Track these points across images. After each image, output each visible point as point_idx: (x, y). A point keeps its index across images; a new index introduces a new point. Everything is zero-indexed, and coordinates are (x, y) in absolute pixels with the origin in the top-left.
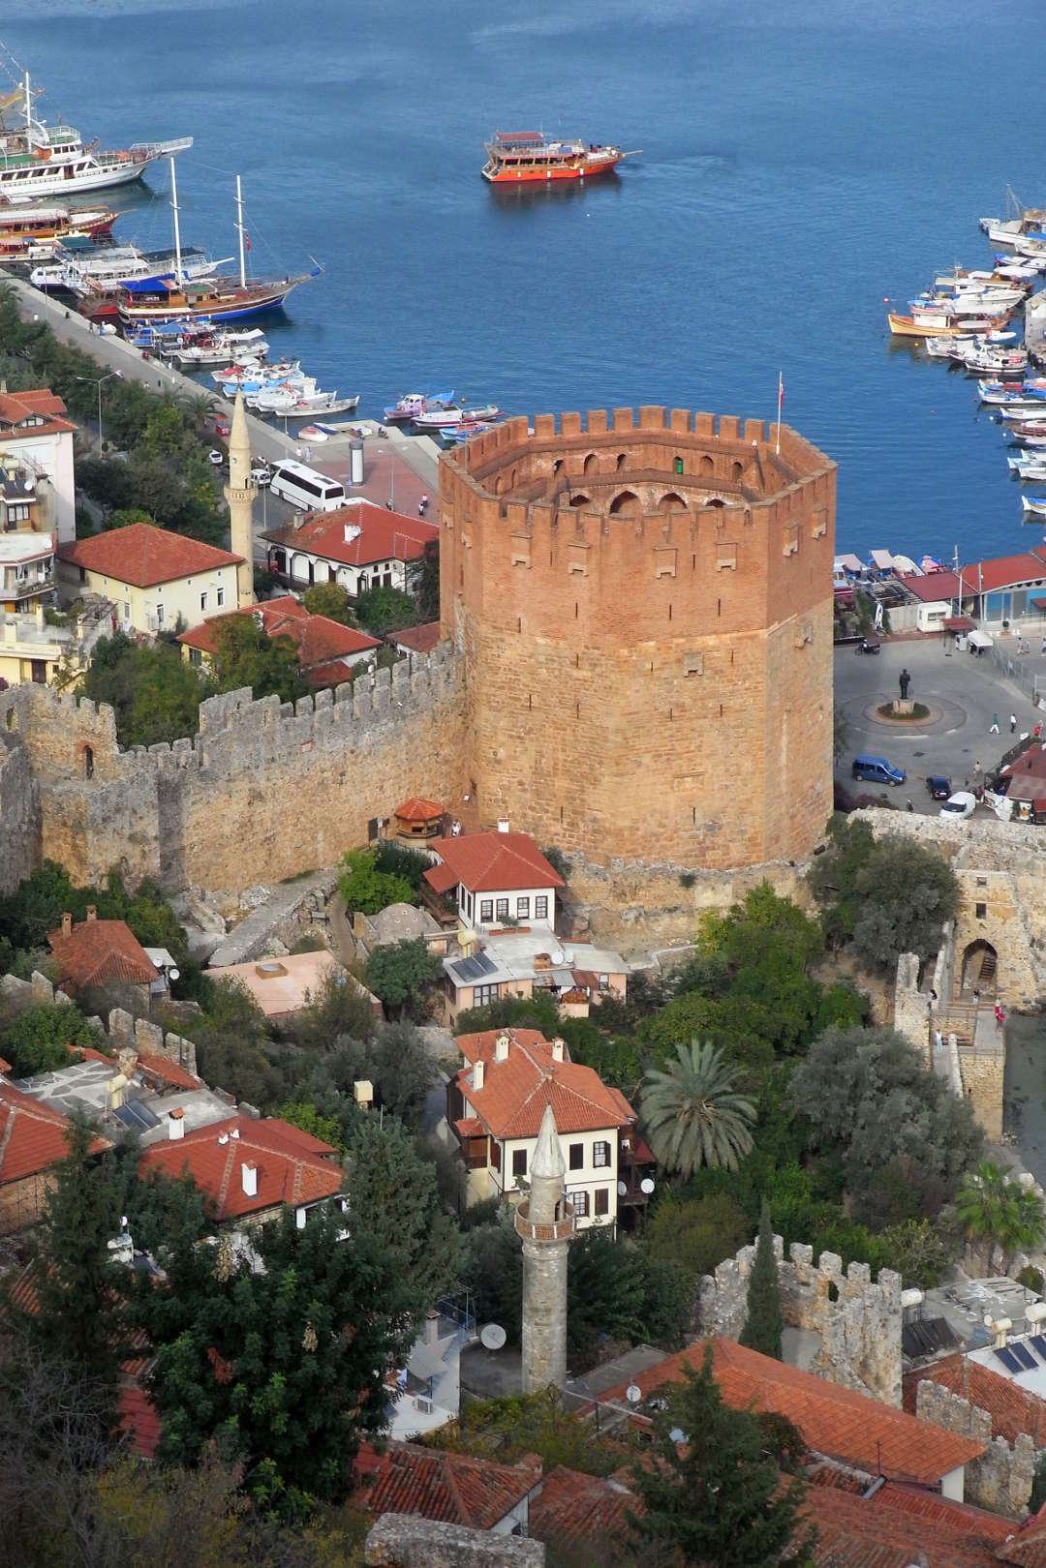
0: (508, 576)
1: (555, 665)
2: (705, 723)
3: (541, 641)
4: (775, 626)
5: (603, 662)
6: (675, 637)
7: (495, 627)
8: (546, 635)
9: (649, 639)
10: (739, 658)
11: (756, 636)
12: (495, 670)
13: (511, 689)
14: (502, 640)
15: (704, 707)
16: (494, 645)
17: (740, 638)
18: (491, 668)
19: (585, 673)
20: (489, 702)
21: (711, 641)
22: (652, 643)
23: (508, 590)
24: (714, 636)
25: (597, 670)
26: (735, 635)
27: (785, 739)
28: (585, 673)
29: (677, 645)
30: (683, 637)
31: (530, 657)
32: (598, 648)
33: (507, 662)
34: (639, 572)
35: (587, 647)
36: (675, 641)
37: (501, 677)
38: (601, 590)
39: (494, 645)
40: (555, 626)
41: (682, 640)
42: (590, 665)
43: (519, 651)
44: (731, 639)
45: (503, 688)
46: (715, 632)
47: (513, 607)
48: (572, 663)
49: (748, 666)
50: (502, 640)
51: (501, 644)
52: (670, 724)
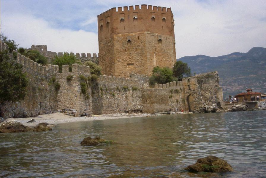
2: (133, 52)
4: (149, 32)
6: (125, 33)
9: (120, 33)
10: (140, 38)
11: (143, 33)
15: (133, 49)
17: (140, 33)
21: (134, 34)
22: (121, 34)
24: (134, 33)
26: (139, 33)
27: (155, 60)
29: (126, 35)
30: (127, 33)
34: (117, 19)
36: (126, 34)
41: (127, 34)
44: (138, 33)
46: (134, 32)
49: (142, 40)
52: (126, 52)
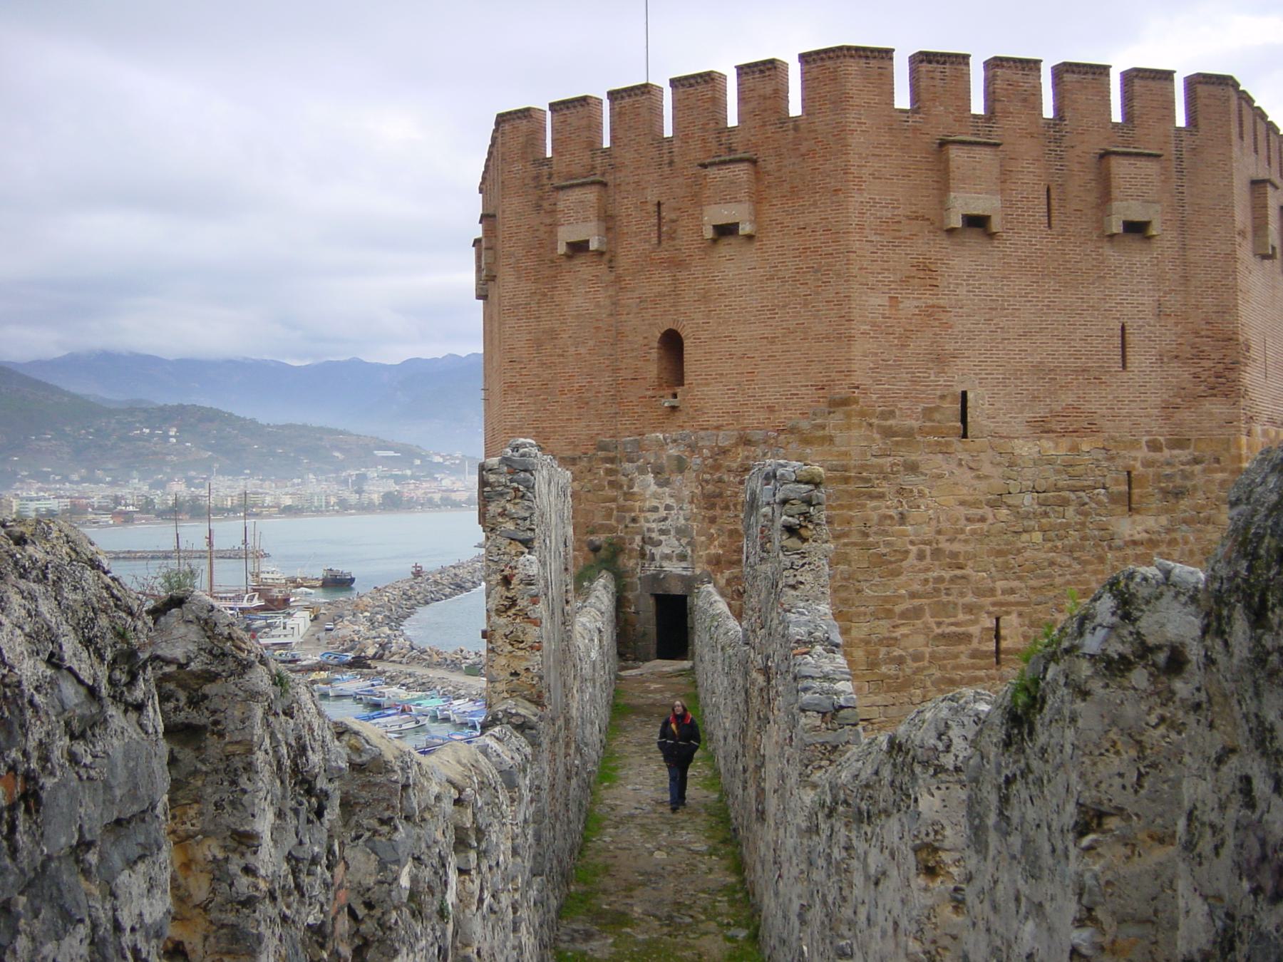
0: (926, 272)
1: (1070, 512)
3: (1025, 449)
5: (1199, 480)
7: (888, 433)
8: (1041, 428)
12: (887, 564)
13: (943, 609)
14: (913, 468)
16: (884, 487)
18: (880, 560)
19: (1151, 522)
20: (873, 665)
23: (930, 312)
25: (1184, 503)
28: (1151, 522)
31: (993, 505)
32: (1179, 443)
33: (928, 531)
35: (1154, 446)
37: (908, 581)
38: (1186, 279)
39: (884, 487)
40: (1068, 398)
42: (1165, 492)
43: (964, 493)
45: (917, 612)
47: (940, 360)
48: (1114, 499)
50: (913, 468)
51: (909, 480)
